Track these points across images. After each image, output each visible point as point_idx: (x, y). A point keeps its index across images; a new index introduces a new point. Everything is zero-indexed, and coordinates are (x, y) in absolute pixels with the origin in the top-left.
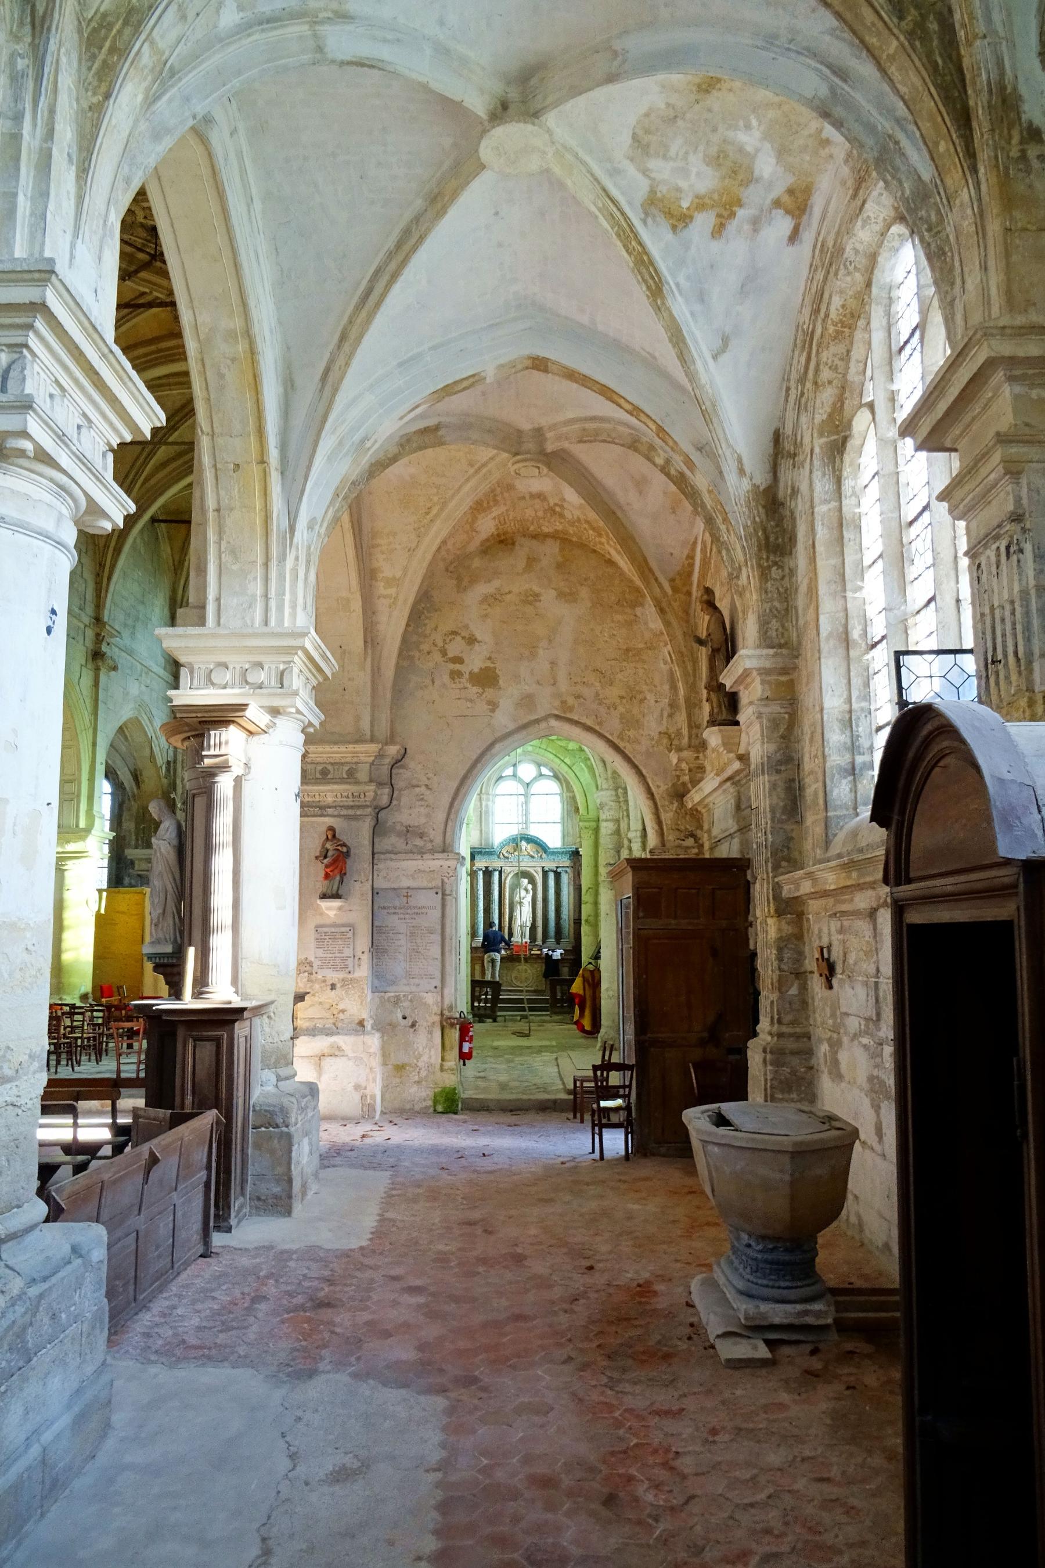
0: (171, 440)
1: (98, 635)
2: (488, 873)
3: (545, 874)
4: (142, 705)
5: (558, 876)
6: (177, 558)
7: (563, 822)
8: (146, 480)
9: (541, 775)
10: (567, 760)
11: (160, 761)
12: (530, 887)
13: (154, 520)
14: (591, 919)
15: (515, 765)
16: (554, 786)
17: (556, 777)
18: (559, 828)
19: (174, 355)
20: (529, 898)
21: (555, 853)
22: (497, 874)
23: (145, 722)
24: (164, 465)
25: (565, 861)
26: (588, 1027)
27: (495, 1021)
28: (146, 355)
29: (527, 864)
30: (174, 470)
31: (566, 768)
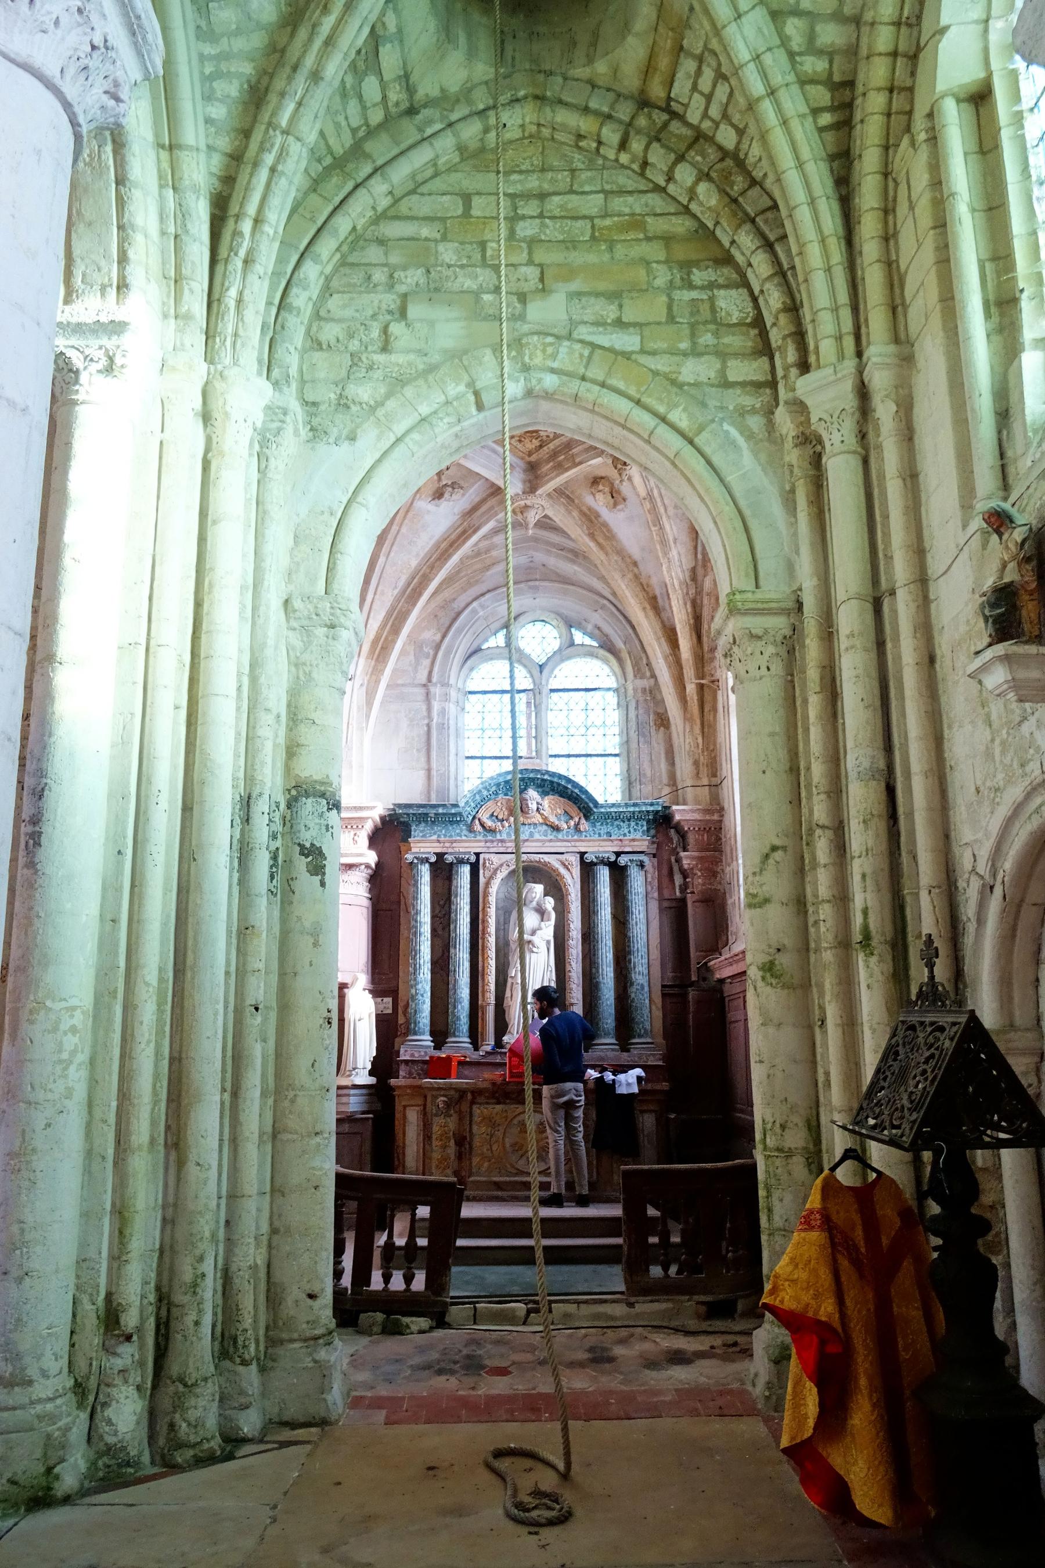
2: (443, 870)
3: (588, 869)
5: (619, 873)
7: (627, 752)
9: (572, 644)
10: (677, 416)
12: (549, 903)
14: (786, 961)
15: (506, 626)
16: (598, 672)
17: (608, 647)
18: (615, 766)
20: (548, 931)
21: (613, 817)
22: (466, 870)
25: (638, 838)
26: (871, 1499)
27: (441, 1322)
29: (537, 844)
31: (676, 442)
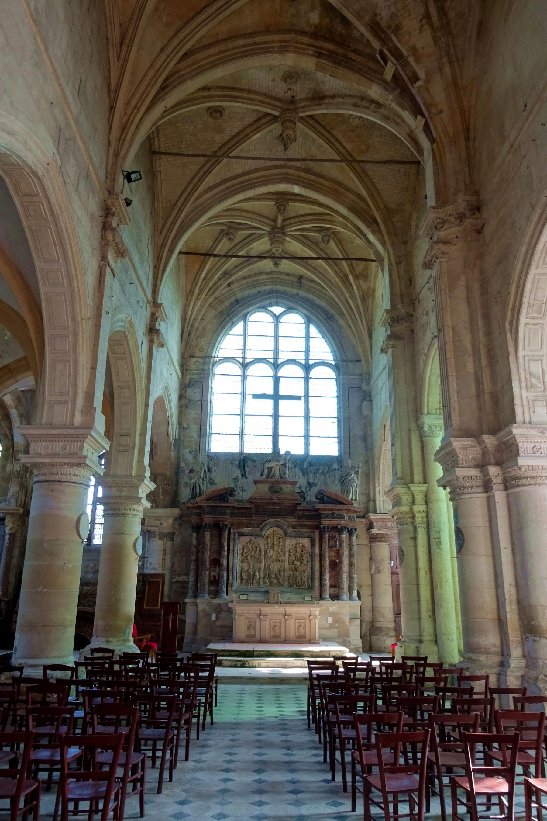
0: (230, 155)
1: (153, 315)
4: (166, 388)
6: (189, 288)
8: (197, 199)
11: (171, 439)
13: (180, 253)
19: (269, 48)
23: (167, 403)
24: (211, 188)
28: (244, 46)
30: (220, 192)
